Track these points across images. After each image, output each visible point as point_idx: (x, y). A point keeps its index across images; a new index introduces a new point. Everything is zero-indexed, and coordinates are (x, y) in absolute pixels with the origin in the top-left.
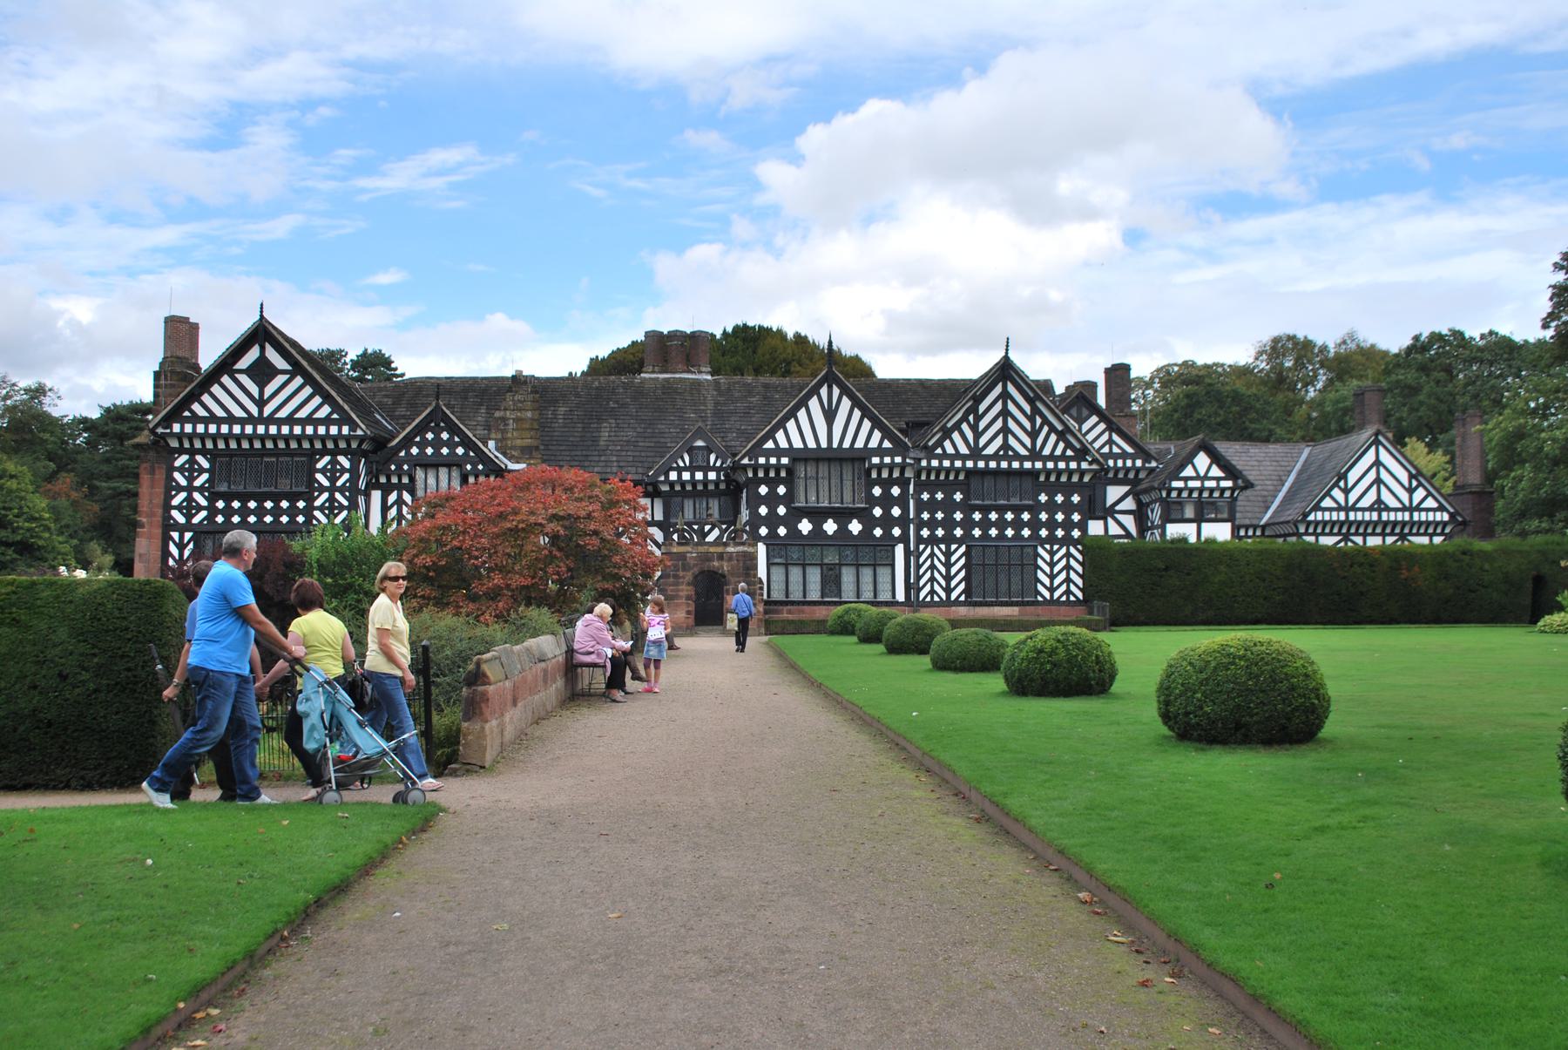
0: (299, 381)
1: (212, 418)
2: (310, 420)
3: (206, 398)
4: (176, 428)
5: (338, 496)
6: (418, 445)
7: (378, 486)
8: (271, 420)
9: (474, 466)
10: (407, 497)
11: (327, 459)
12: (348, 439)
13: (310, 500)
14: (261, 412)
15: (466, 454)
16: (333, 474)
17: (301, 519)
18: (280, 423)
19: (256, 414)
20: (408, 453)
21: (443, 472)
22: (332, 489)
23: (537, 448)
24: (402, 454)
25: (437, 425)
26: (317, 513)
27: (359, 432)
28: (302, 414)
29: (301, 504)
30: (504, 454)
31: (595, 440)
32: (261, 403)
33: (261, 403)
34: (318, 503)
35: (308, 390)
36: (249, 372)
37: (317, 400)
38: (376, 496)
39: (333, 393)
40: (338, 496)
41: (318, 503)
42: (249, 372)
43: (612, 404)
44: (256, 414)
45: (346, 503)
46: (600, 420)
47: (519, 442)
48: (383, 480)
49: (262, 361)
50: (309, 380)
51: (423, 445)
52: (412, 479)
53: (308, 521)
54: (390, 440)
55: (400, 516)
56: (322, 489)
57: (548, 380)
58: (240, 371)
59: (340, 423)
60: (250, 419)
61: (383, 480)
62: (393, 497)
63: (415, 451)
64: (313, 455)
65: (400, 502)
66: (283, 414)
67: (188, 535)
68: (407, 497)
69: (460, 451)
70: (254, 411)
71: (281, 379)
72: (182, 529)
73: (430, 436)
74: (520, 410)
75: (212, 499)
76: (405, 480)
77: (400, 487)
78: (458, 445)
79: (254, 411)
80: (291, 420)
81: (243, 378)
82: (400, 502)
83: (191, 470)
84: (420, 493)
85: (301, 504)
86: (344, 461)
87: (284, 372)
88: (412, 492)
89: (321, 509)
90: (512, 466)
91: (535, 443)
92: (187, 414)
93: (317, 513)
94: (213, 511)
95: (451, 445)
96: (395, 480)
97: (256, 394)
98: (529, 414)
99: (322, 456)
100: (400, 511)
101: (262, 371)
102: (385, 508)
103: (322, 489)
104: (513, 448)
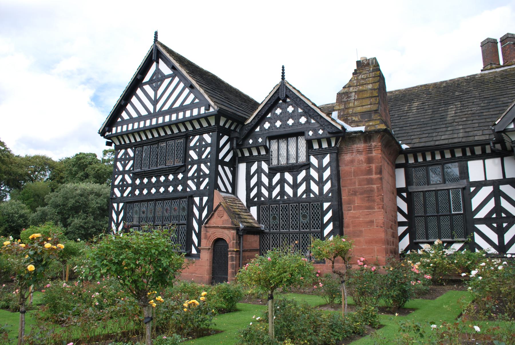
0: (177, 79)
1: (132, 120)
2: (183, 108)
3: (129, 107)
4: (114, 130)
5: (203, 166)
6: (269, 120)
7: (243, 159)
8: (162, 113)
9: (315, 131)
10: (265, 166)
11: (197, 137)
12: (206, 118)
13: (185, 172)
14: (155, 109)
15: (308, 122)
16: (200, 149)
17: (180, 188)
18: (162, 113)
19: (152, 111)
20: (262, 129)
21: (292, 141)
22: (199, 162)
23: (376, 111)
24: (258, 129)
25: (284, 101)
26: (190, 182)
27: (211, 110)
28: (177, 105)
29: (180, 176)
30: (346, 121)
31: (443, 118)
32: (155, 102)
33: (155, 102)
34: (190, 174)
35: (182, 85)
36: (150, 83)
37: (187, 91)
38: (242, 168)
39: (194, 83)
40: (203, 166)
41: (190, 174)
42: (150, 83)
43: (457, 94)
44: (152, 111)
45: (207, 172)
46: (447, 104)
47: (359, 109)
48: (247, 154)
49: (158, 71)
50: (183, 79)
51: (272, 121)
52: (268, 150)
53: (184, 190)
54: (246, 119)
55: (259, 183)
56: (193, 162)
57: (406, 90)
58: (146, 83)
59: (198, 106)
60: (150, 116)
61: (247, 154)
62: (254, 168)
63: (267, 125)
64: (187, 137)
65: (260, 171)
66: (166, 108)
67: (121, 205)
68: (265, 166)
69: (303, 120)
70: (151, 108)
71: (167, 81)
72: (118, 201)
73: (278, 111)
74: (362, 85)
75: (133, 179)
76: (263, 152)
77: (259, 159)
78: (301, 115)
79: (151, 108)
80: (171, 111)
81: (147, 88)
82: (260, 171)
83: (125, 160)
84: (275, 162)
85: (180, 176)
86: (207, 138)
87: (168, 76)
88: (268, 161)
89: (192, 178)
90: (350, 129)
91: (374, 107)
92: (119, 120)
93: (190, 182)
94: (134, 187)
95: (294, 116)
96: (255, 153)
97: (152, 96)
98: (370, 86)
99: (194, 136)
100: (259, 178)
101: (158, 79)
102: (249, 177)
103: (193, 162)
104: (355, 114)
